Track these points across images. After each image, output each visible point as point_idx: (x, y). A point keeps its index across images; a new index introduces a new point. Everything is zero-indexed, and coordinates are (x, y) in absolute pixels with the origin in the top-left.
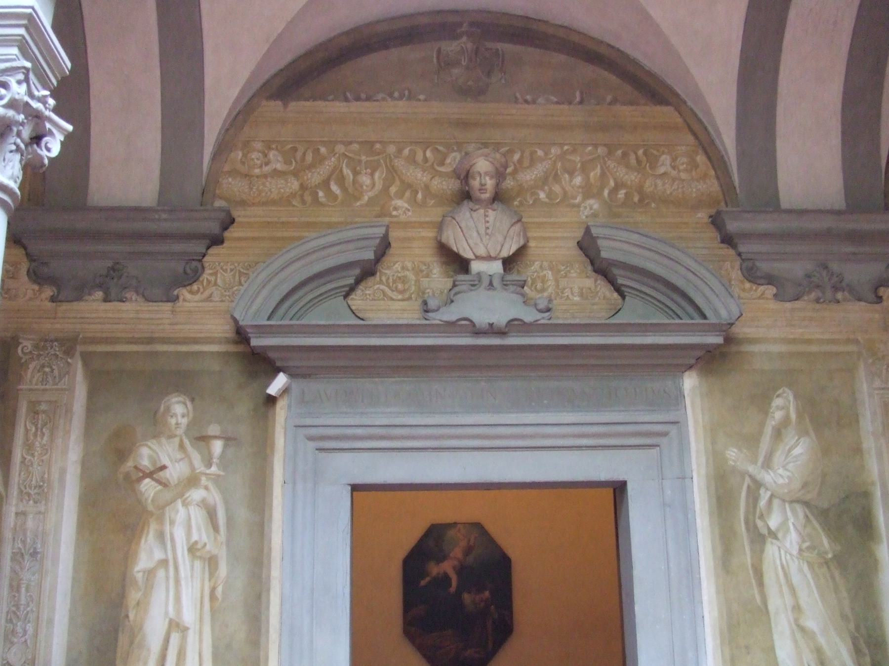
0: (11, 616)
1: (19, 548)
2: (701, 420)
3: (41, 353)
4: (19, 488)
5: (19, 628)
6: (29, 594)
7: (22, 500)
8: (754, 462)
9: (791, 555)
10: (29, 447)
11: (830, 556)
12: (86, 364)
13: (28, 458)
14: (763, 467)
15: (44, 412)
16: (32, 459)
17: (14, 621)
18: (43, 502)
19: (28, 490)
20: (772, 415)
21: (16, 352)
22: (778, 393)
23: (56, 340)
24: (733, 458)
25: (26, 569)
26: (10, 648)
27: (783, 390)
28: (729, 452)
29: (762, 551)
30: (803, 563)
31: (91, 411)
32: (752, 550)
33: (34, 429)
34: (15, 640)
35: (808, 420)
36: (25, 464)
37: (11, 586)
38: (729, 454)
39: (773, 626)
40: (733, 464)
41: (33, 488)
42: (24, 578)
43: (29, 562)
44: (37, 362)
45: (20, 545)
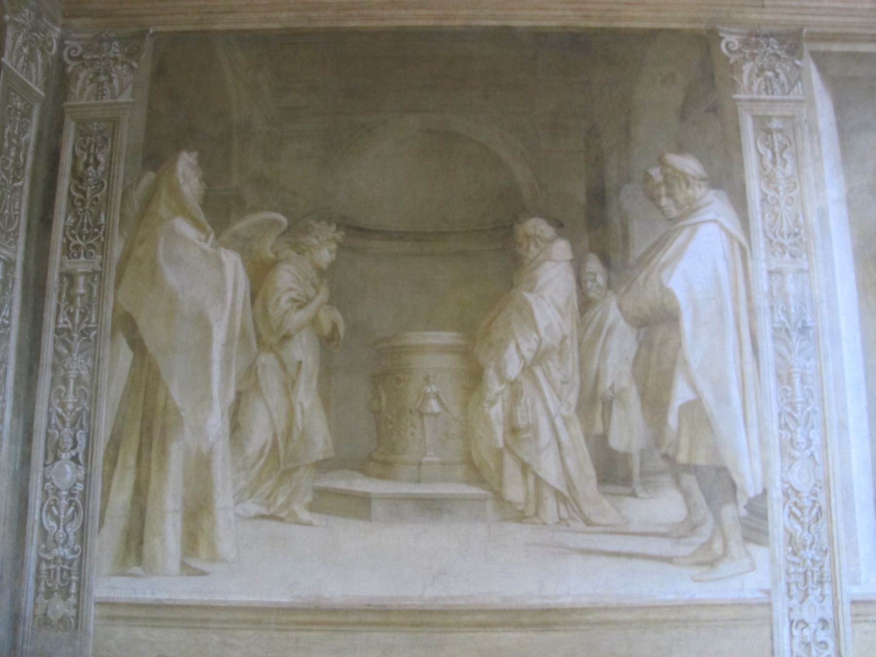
0: (785, 420)
1: (781, 322)
3: (755, 51)
4: (766, 236)
5: (799, 436)
6: (805, 387)
7: (773, 253)
10: (769, 179)
12: (822, 69)
13: (771, 193)
15: (779, 131)
16: (777, 196)
17: (792, 427)
18: (804, 256)
19: (780, 239)
21: (720, 49)
23: (772, 35)
25: (797, 351)
26: (790, 467)
31: (844, 132)
33: (770, 154)
34: (797, 454)
36: (768, 203)
37: (778, 376)
41: (785, 236)
42: (797, 365)
43: (798, 342)
44: (752, 63)
45: (782, 318)
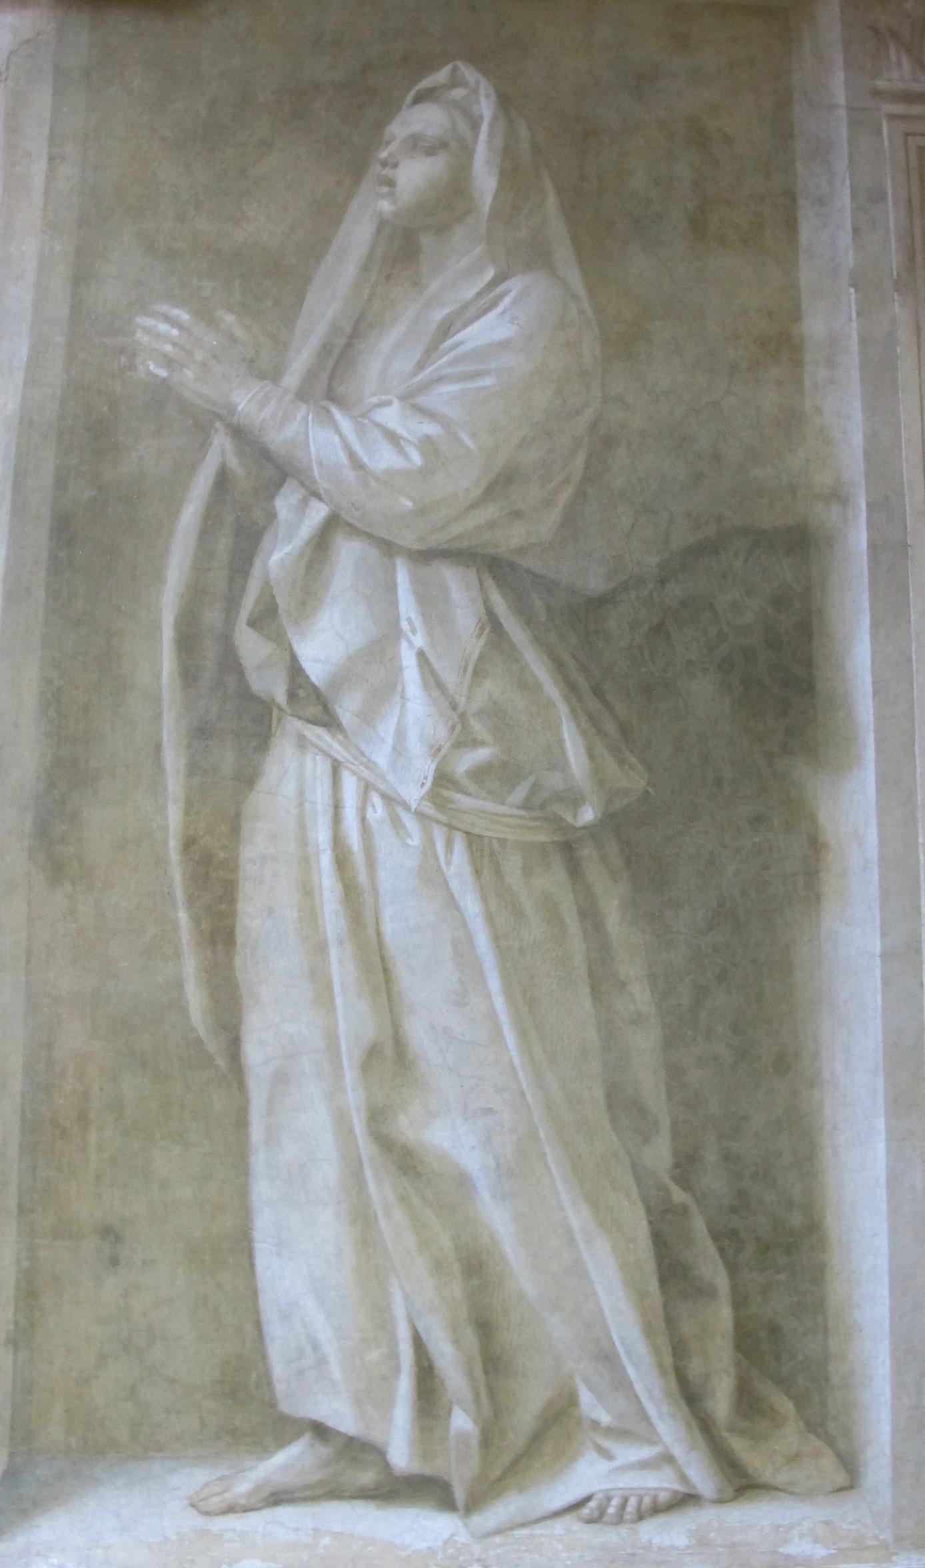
2: (38, 178)
8: (273, 375)
9: (390, 800)
11: (588, 815)
14: (302, 395)
20: (387, 172)
22: (426, 83)
24: (168, 348)
27: (455, 69)
28: (149, 322)
29: (248, 779)
30: (449, 844)
32: (193, 769)
35: (552, 201)
38: (147, 330)
39: (257, 1132)
40: (163, 373)
